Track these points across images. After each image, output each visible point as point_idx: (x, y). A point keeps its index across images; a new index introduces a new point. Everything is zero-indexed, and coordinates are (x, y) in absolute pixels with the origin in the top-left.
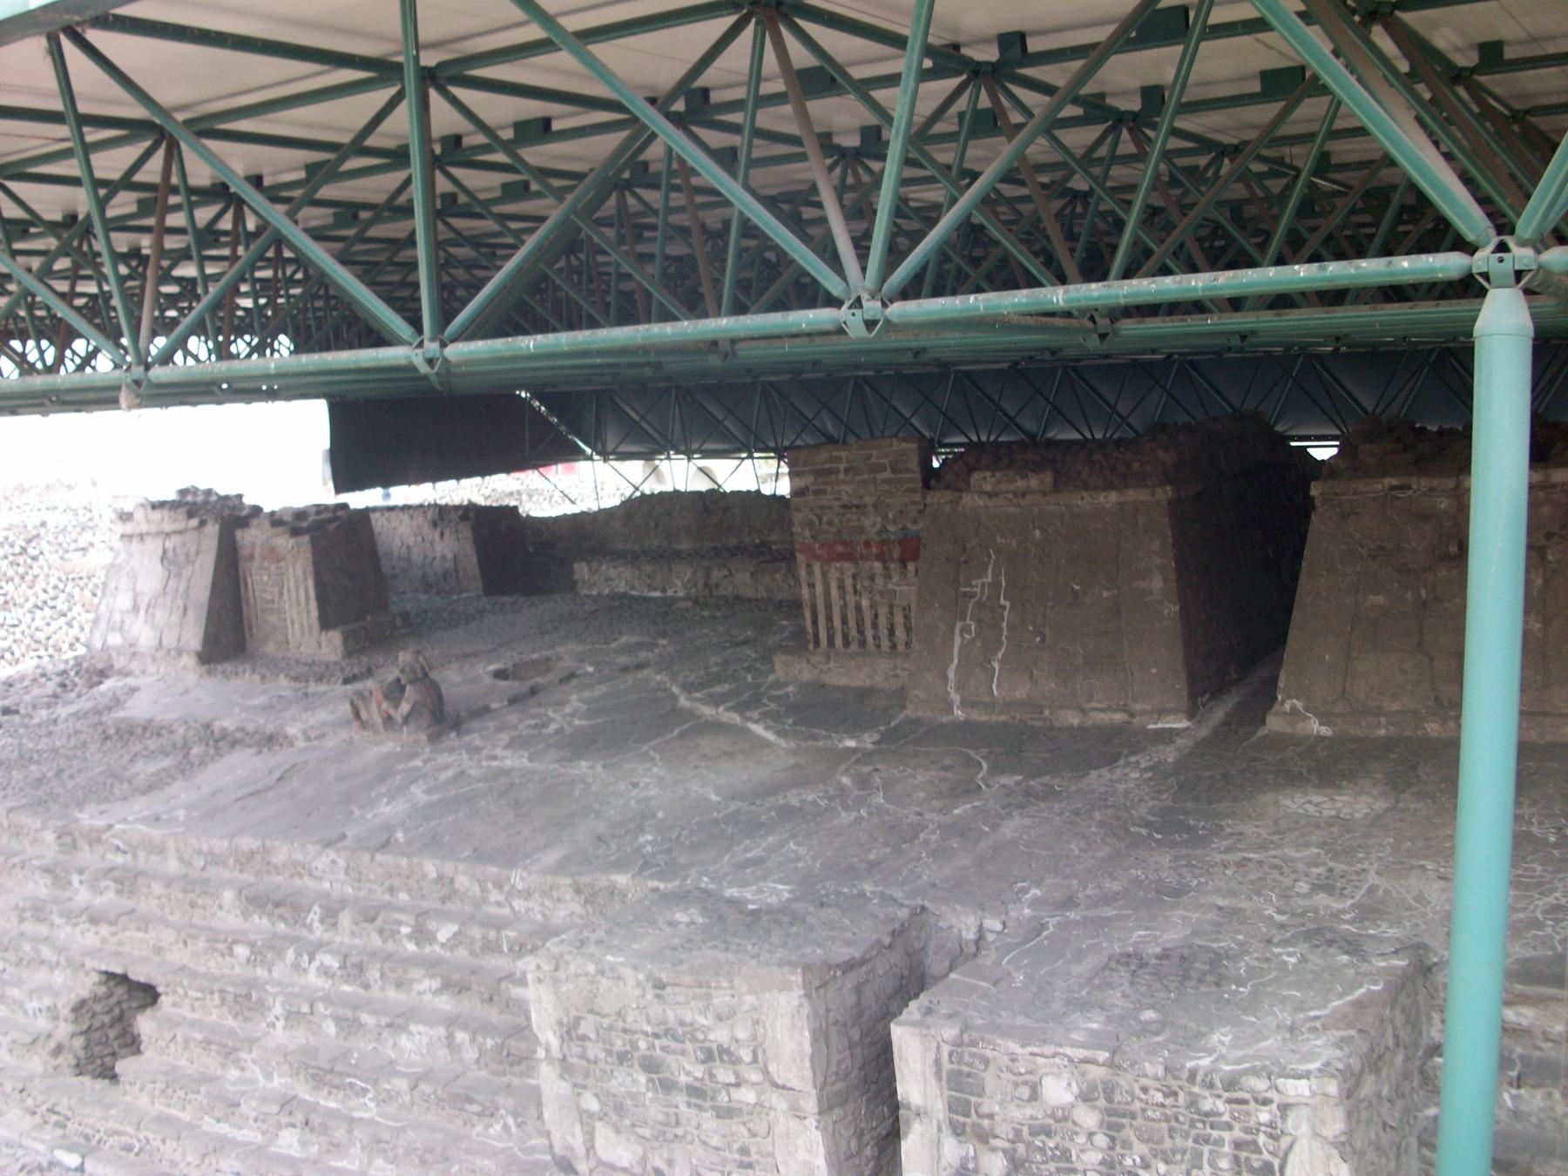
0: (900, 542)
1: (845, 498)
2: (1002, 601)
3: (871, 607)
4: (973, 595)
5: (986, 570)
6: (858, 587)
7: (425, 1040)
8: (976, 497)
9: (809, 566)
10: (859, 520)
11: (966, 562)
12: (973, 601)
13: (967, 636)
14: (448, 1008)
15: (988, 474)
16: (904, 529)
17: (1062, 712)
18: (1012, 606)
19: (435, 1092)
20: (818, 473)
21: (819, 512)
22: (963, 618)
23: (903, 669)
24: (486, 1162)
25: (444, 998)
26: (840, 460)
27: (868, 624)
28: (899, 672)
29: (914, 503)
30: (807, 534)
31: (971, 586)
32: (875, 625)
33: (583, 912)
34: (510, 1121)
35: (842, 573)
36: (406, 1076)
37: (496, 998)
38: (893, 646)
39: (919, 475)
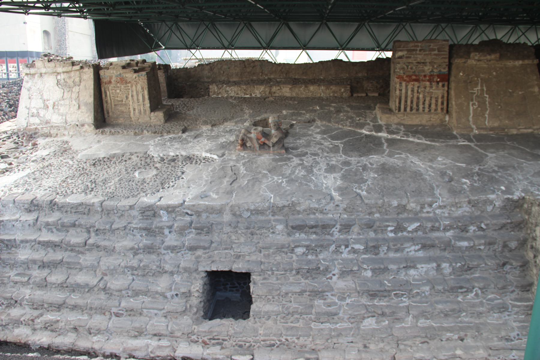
1: (419, 60)
2: (485, 95)
3: (423, 97)
4: (475, 93)
6: (419, 91)
7: (424, 269)
9: (401, 83)
11: (470, 82)
13: (475, 107)
14: (422, 255)
15: (477, 54)
16: (440, 71)
17: (511, 130)
18: (489, 97)
19: (444, 289)
20: (408, 51)
21: (407, 64)
22: (472, 100)
24: (481, 308)
25: (420, 252)
27: (421, 103)
29: (445, 62)
30: (402, 72)
32: (424, 104)
33: (470, 210)
34: (479, 292)
36: (424, 284)
37: (448, 248)
38: (430, 111)
39: (447, 53)
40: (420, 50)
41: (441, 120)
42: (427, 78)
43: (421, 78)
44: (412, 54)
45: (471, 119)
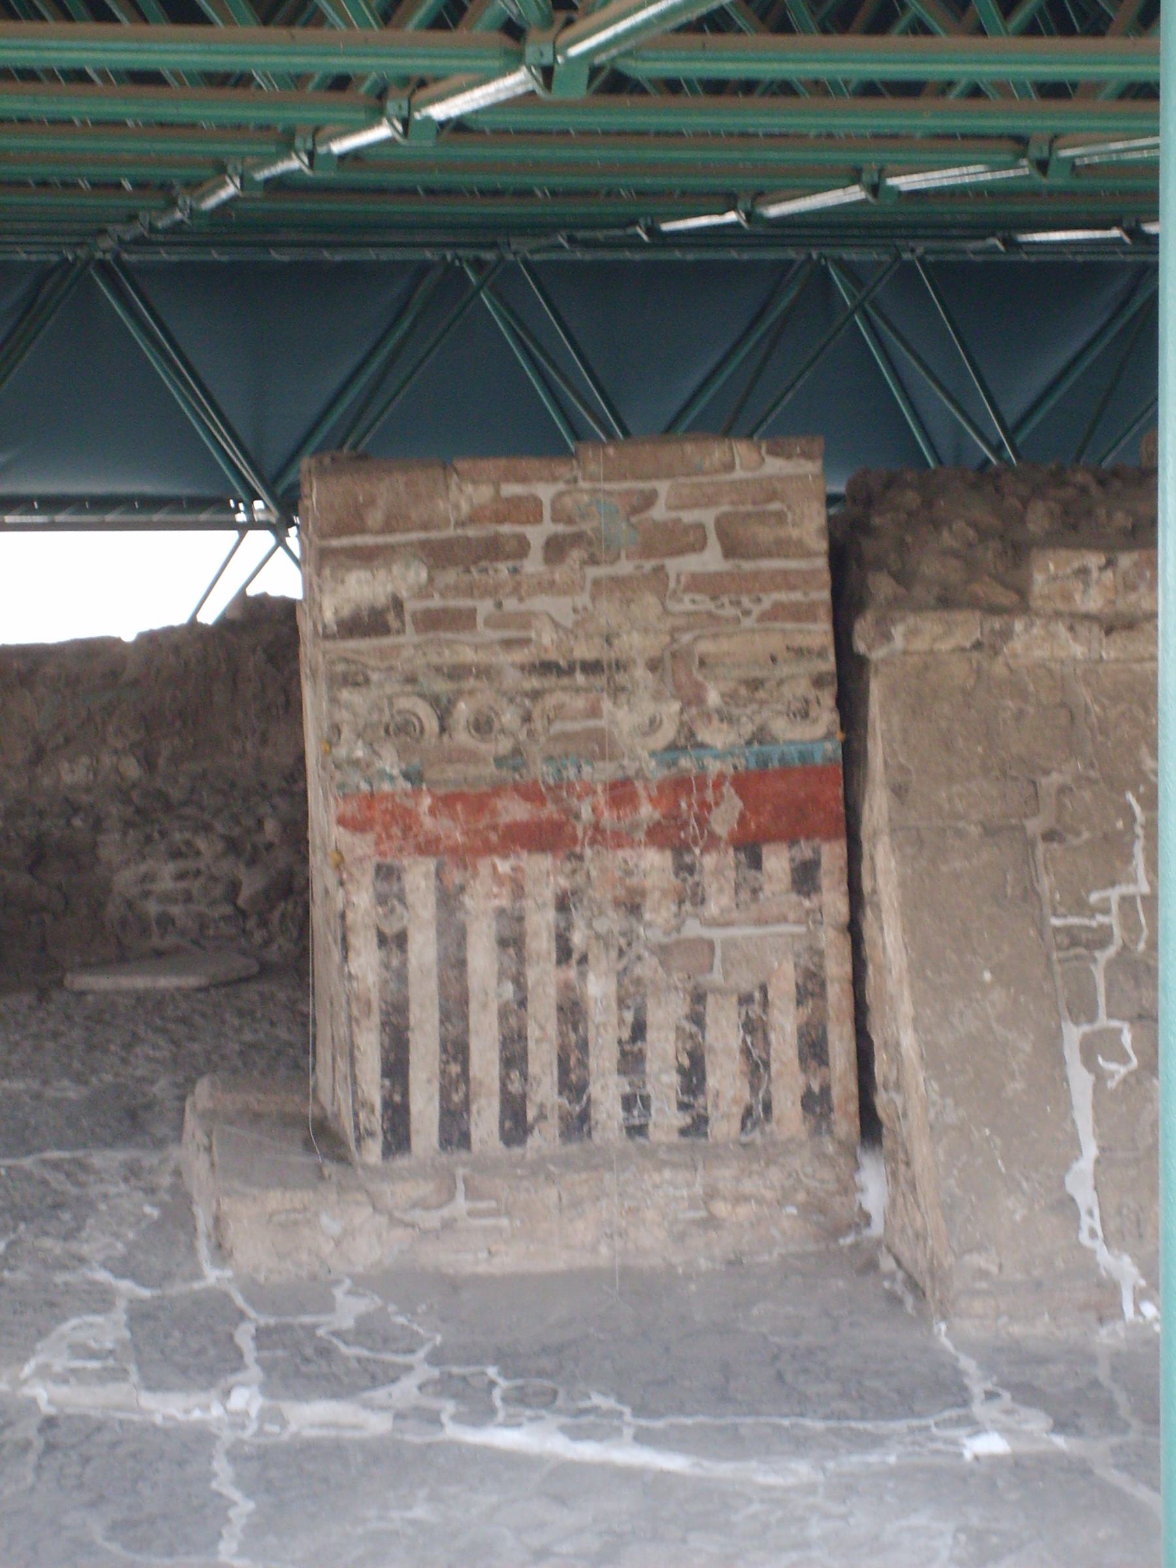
0: (741, 783)
3: (621, 1003)
4: (1102, 938)
5: (1129, 858)
6: (578, 938)
8: (1061, 629)
9: (387, 873)
10: (594, 712)
12: (1104, 956)
13: (1119, 1070)
15: (1094, 560)
16: (761, 736)
21: (442, 686)
23: (740, 1199)
26: (530, 511)
28: (721, 1208)
29: (800, 653)
30: (389, 762)
31: (1081, 907)
35: (518, 891)
39: (822, 563)
40: (555, 549)
41: (815, 1207)
42: (647, 812)
43: (586, 812)
44: (469, 591)
45: (1084, 1195)
